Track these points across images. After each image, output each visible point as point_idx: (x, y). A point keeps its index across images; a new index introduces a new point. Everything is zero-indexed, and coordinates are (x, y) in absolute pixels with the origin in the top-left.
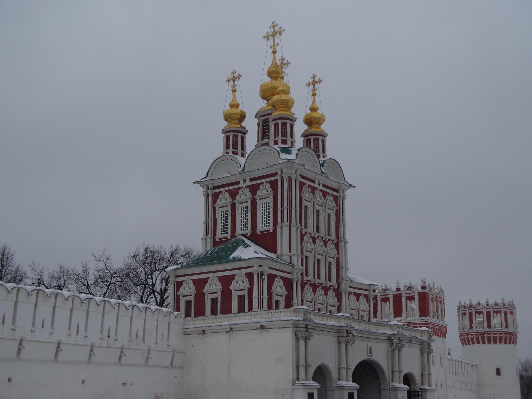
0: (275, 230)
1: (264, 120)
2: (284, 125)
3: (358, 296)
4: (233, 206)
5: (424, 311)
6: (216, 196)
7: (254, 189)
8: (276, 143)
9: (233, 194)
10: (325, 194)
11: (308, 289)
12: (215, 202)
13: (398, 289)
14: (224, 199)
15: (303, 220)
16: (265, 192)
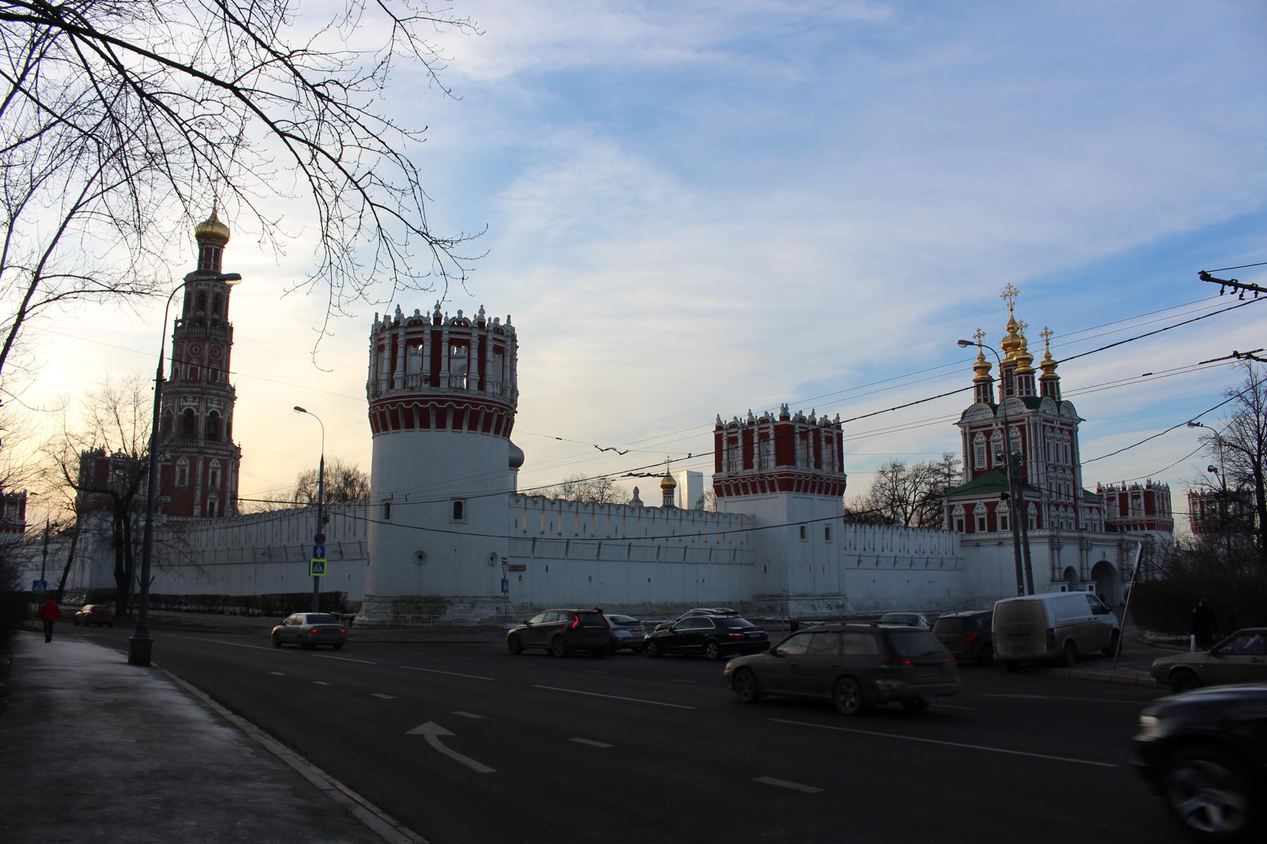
0: (1025, 464)
1: (1007, 369)
2: (1027, 378)
3: (1091, 508)
4: (988, 444)
5: (1150, 509)
6: (973, 435)
7: (1006, 430)
8: (1021, 393)
9: (988, 434)
10: (1062, 430)
11: (1053, 508)
12: (972, 440)
13: (1124, 489)
14: (980, 438)
15: (1047, 457)
16: (1015, 433)
